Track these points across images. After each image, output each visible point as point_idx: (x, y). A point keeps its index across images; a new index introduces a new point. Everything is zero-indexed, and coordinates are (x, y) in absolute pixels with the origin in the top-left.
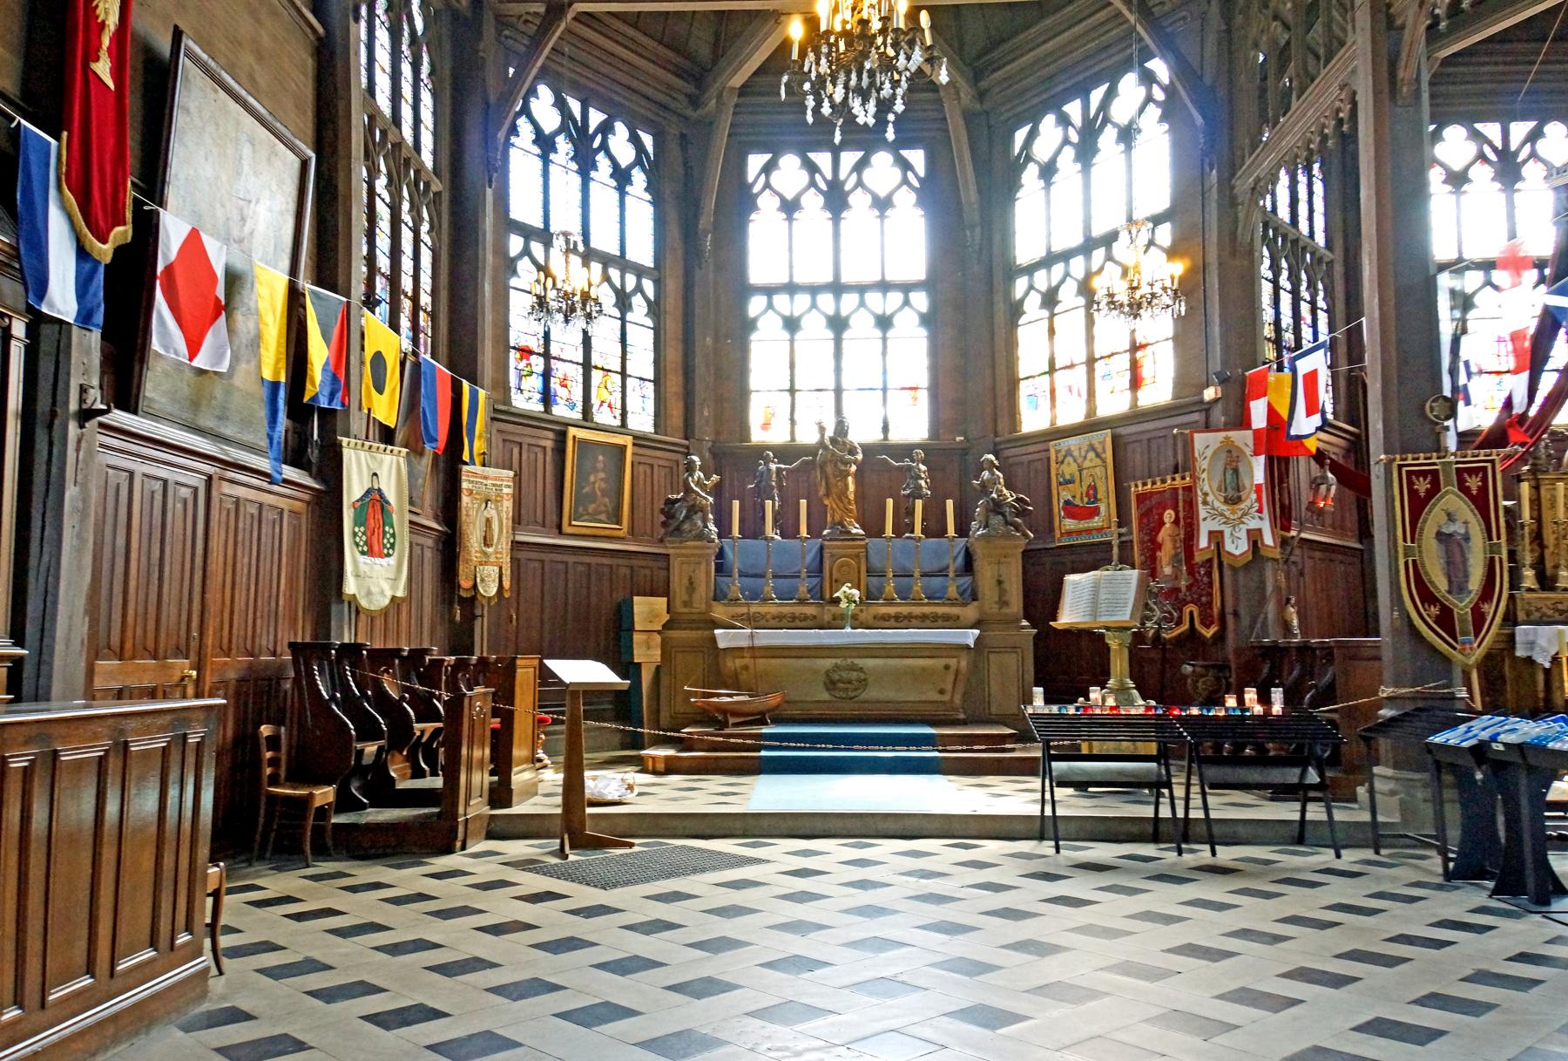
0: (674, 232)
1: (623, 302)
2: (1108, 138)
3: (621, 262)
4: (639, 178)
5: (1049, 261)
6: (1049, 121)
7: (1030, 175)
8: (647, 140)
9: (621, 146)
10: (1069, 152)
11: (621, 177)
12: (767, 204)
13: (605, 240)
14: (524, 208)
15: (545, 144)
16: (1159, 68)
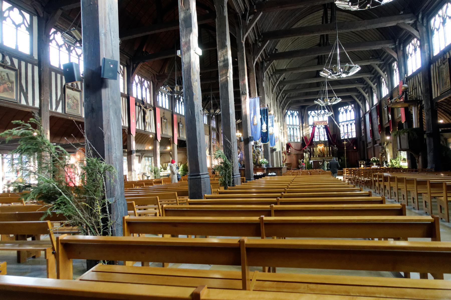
0: (301, 122)
1: (296, 129)
2: (348, 111)
3: (296, 125)
4: (297, 116)
5: (343, 122)
6: (342, 108)
7: (341, 113)
8: (298, 112)
9: (296, 114)
10: (344, 112)
11: (296, 117)
12: (311, 116)
13: (295, 124)
14: (288, 123)
15: (289, 116)
16: (353, 105)
